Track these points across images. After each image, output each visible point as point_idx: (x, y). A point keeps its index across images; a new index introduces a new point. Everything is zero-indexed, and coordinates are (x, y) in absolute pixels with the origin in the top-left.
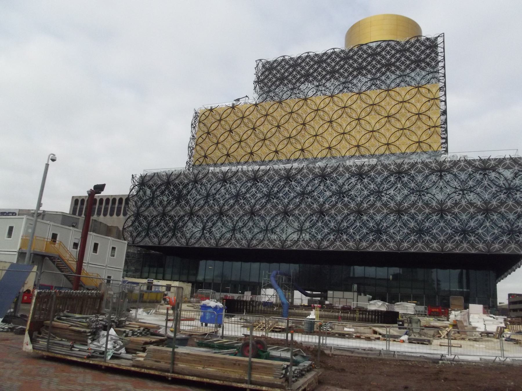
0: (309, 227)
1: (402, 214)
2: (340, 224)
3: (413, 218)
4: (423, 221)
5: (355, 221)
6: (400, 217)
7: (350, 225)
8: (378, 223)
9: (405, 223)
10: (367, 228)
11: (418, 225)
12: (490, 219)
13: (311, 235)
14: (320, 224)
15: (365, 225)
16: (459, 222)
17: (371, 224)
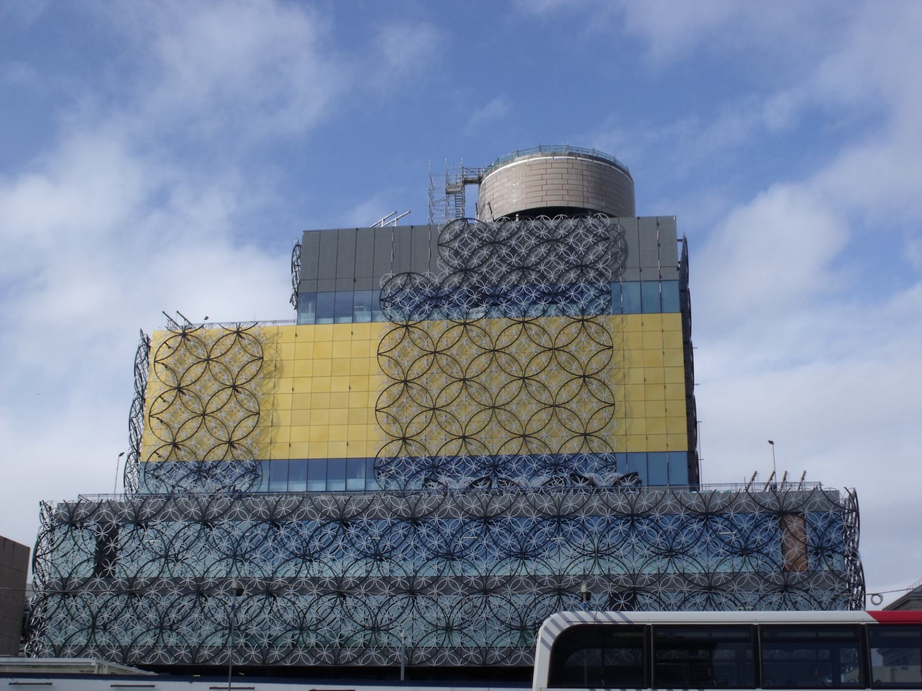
0: (249, 549)
1: (491, 524)
2: (308, 544)
3: (510, 530)
4: (527, 535)
5: (335, 537)
6: (488, 529)
7: (326, 545)
8: (448, 540)
9: (496, 540)
10: (429, 549)
11: (519, 543)
12: (711, 528)
13: (252, 565)
14: (270, 544)
15: (424, 545)
16: (661, 536)
17: (436, 543)
